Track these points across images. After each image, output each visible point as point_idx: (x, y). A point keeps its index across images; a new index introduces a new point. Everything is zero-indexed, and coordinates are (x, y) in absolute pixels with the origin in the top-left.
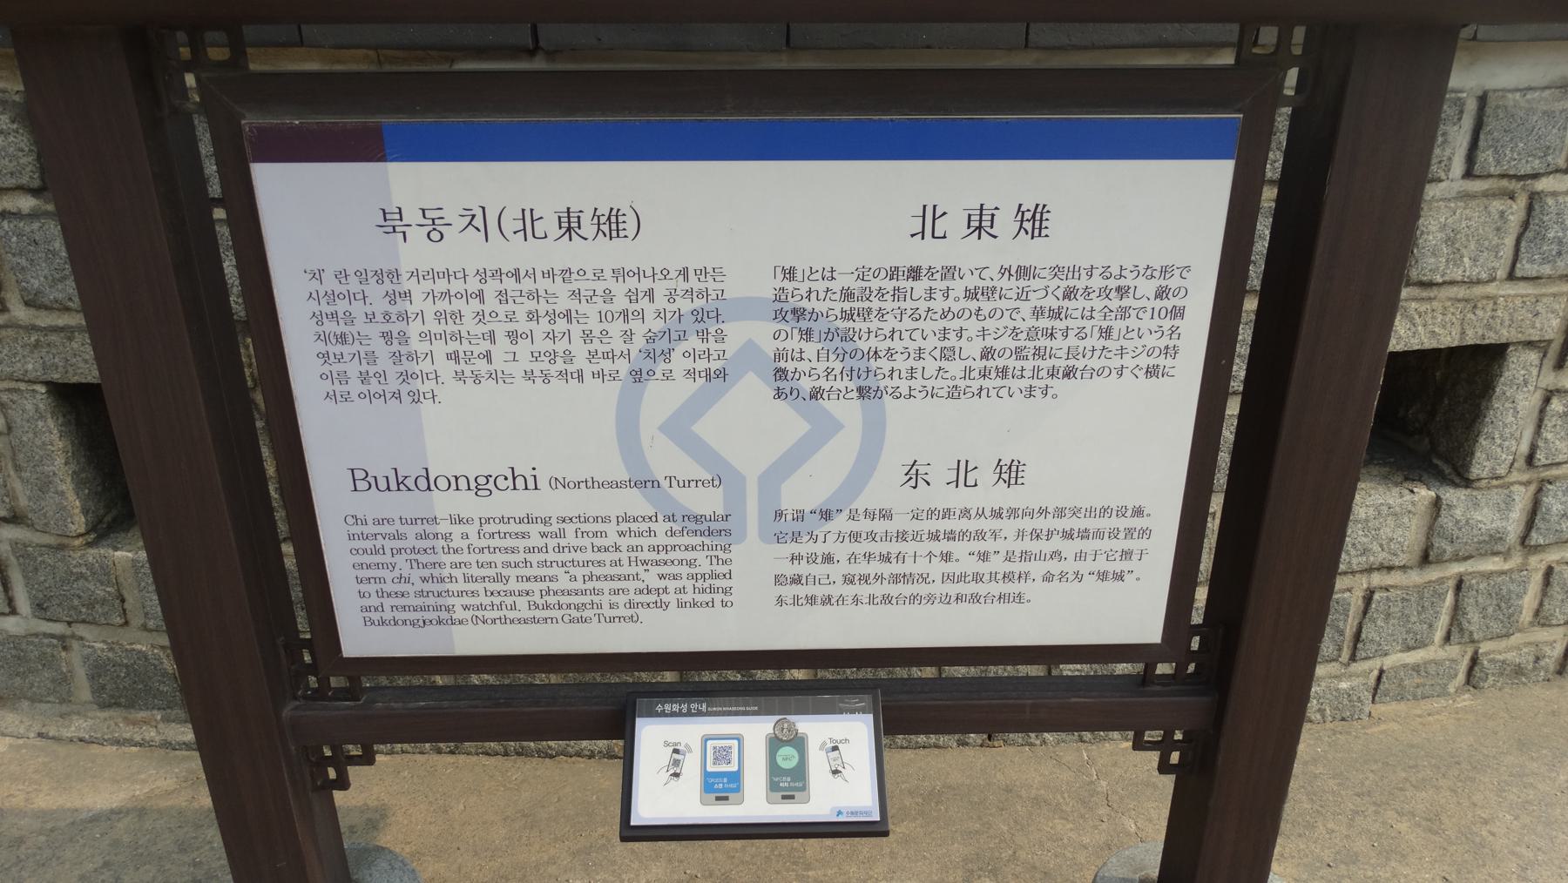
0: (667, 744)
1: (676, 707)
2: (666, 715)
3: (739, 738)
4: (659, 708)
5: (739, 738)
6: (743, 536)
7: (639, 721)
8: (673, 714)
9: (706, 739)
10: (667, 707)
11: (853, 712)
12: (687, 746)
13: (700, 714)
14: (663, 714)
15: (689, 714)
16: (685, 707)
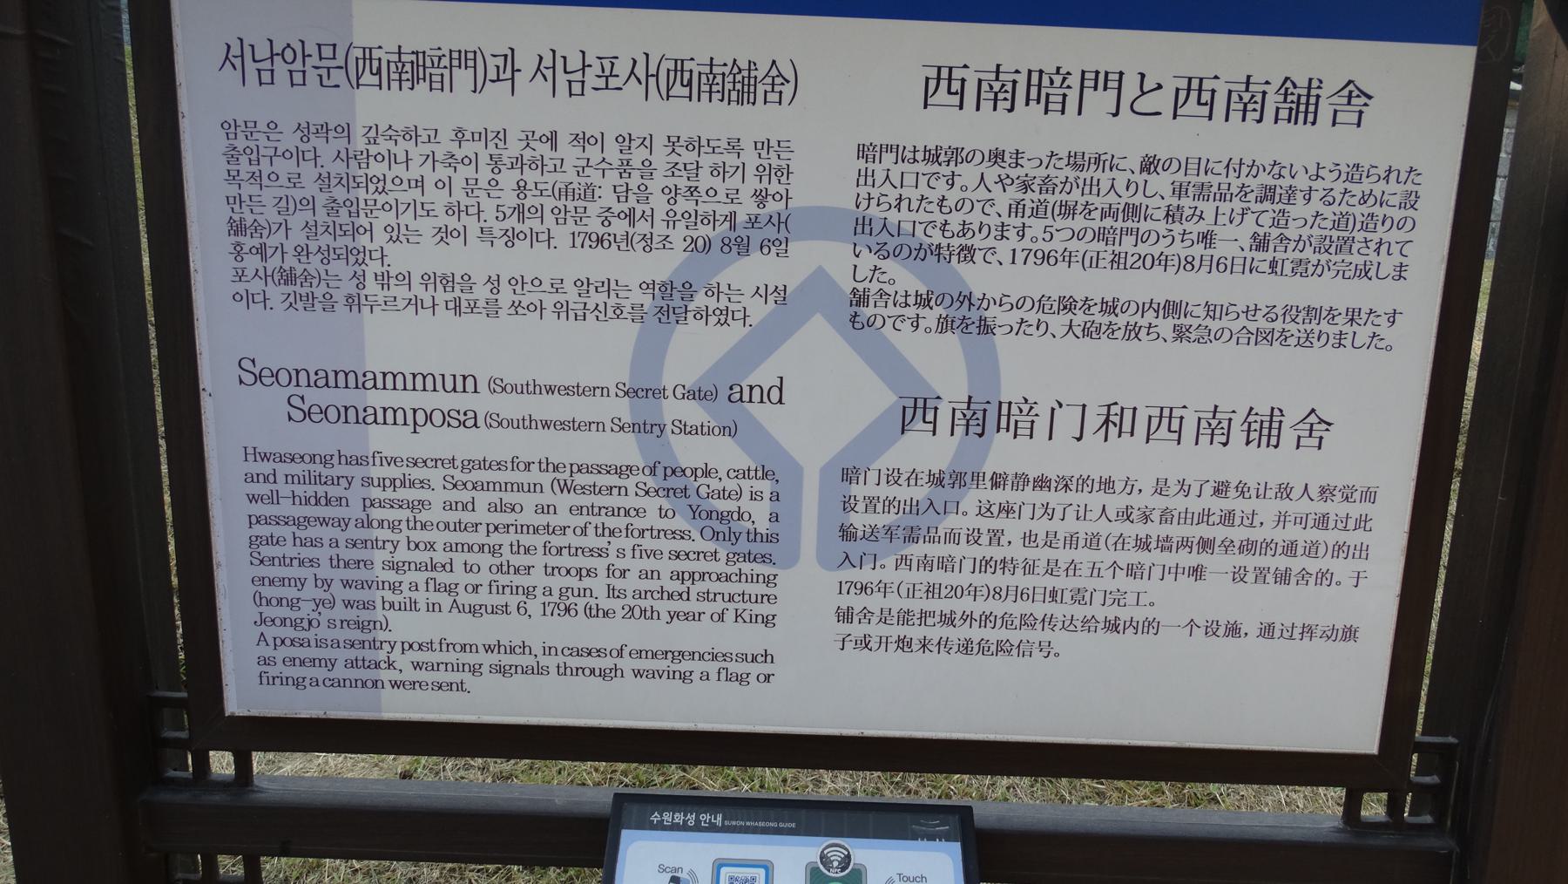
0: (663, 869)
1: (679, 818)
2: (665, 828)
3: (767, 867)
4: (655, 818)
5: (767, 867)
6: (792, 559)
7: (626, 834)
8: (674, 827)
9: (719, 865)
10: (667, 817)
11: (931, 838)
12: (691, 873)
13: (712, 828)
14: (660, 826)
15: (698, 828)
16: (691, 818)
